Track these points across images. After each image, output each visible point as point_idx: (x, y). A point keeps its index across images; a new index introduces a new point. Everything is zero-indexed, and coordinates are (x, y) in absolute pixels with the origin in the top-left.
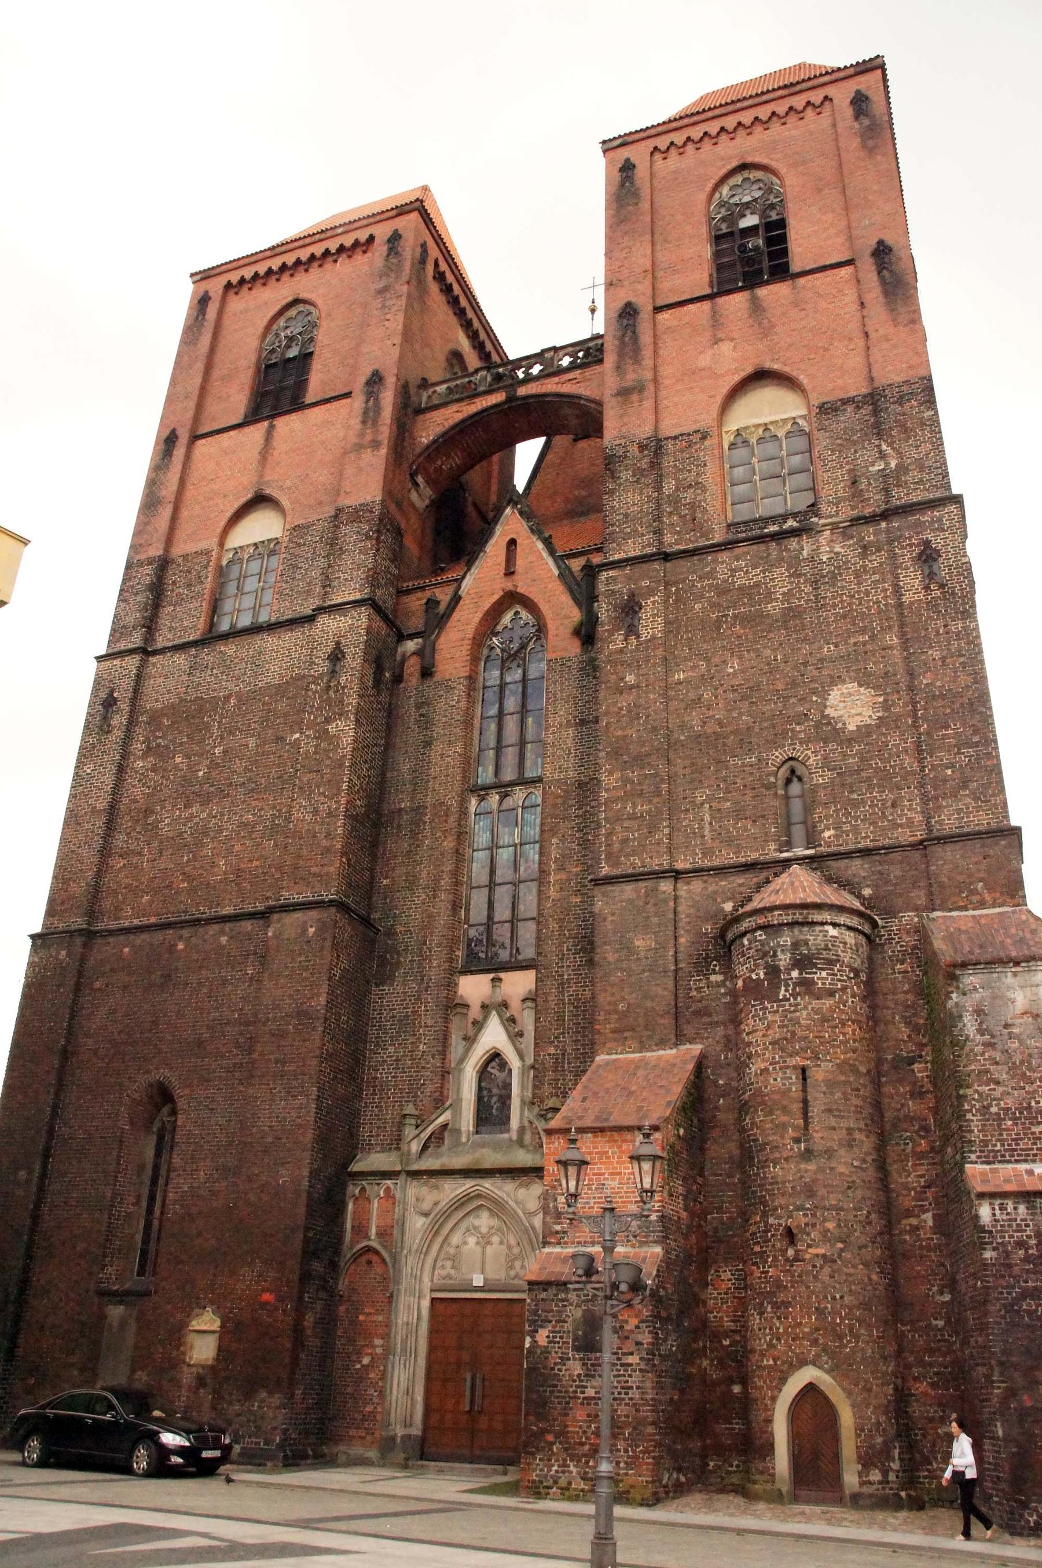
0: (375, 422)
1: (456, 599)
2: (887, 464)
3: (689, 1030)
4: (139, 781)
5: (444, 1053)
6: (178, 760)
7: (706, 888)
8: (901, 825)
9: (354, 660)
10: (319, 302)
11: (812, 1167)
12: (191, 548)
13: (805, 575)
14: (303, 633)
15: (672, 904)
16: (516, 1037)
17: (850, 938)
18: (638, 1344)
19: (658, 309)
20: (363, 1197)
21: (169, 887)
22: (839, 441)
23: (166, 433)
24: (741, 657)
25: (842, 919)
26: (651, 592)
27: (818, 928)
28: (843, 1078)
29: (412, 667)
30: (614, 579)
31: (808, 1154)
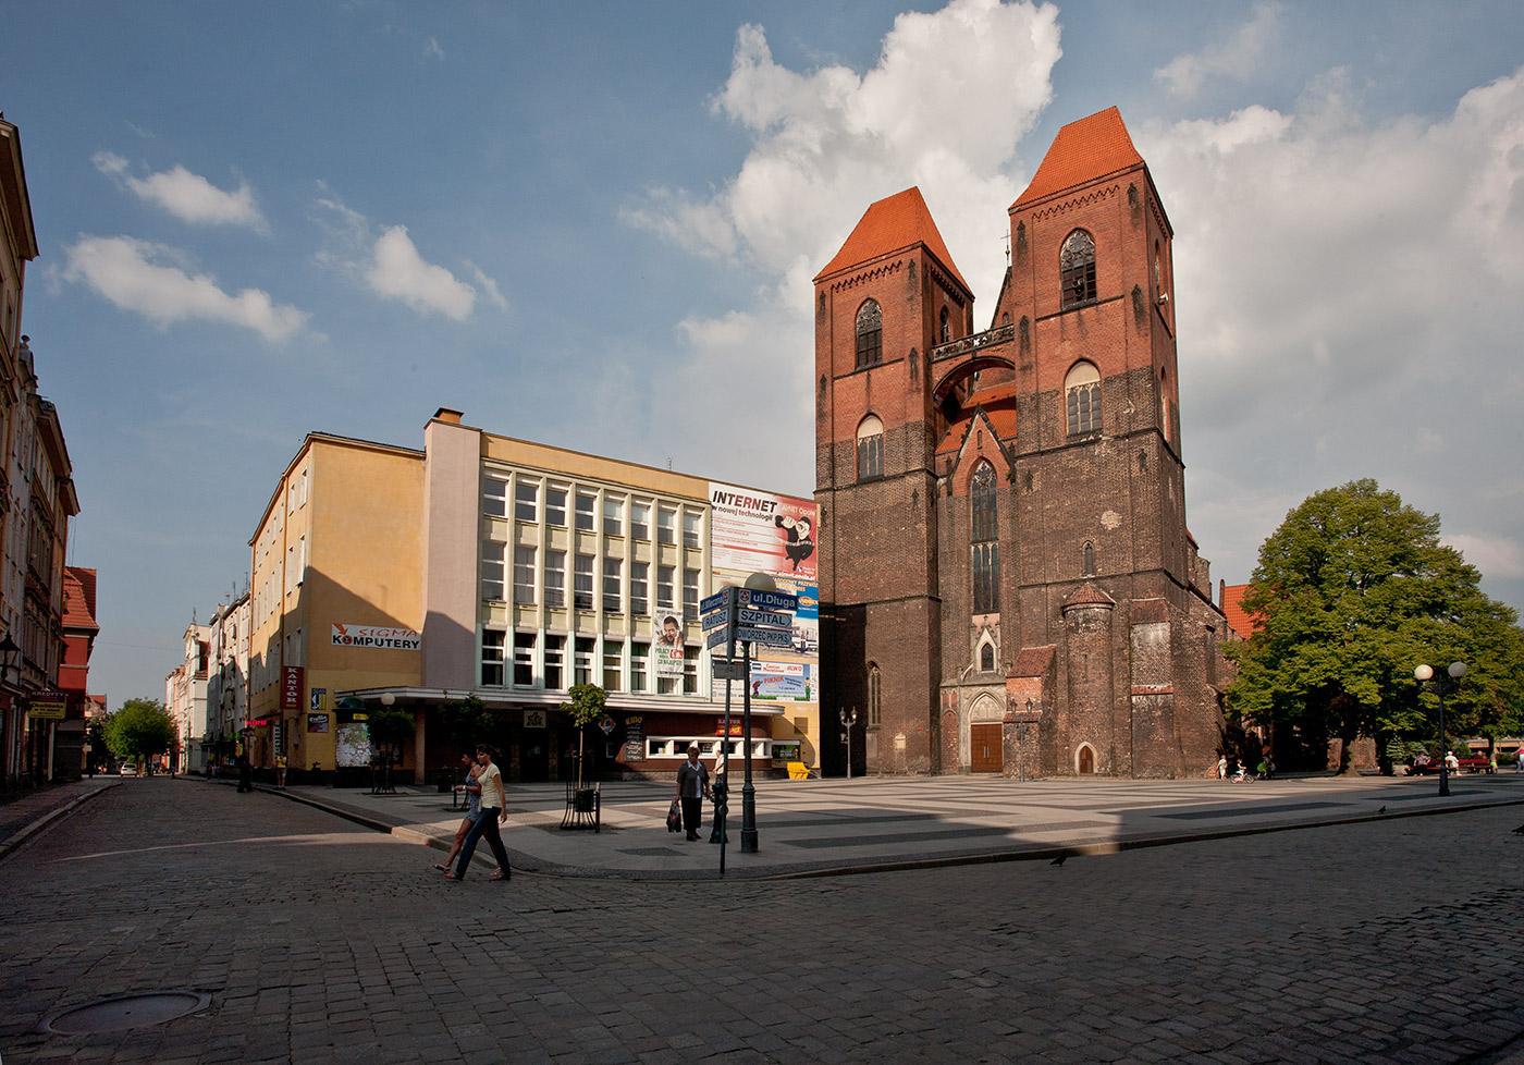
0: (917, 376)
1: (958, 459)
3: (1052, 639)
5: (969, 644)
9: (922, 497)
10: (880, 301)
16: (994, 638)
19: (1037, 320)
23: (820, 377)
25: (1100, 606)
29: (943, 490)
31: (1087, 682)
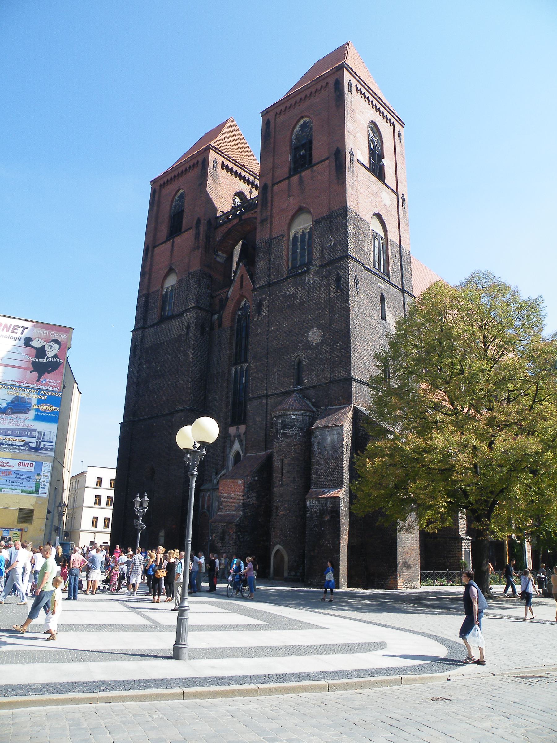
1: (227, 298)
6: (153, 364)
7: (274, 401)
8: (324, 377)
11: (282, 489)
15: (265, 406)
16: (241, 445)
17: (300, 418)
18: (233, 538)
19: (273, 185)
20: (203, 497)
22: (319, 235)
24: (287, 321)
26: (265, 299)
27: (288, 416)
28: (293, 462)
31: (282, 485)
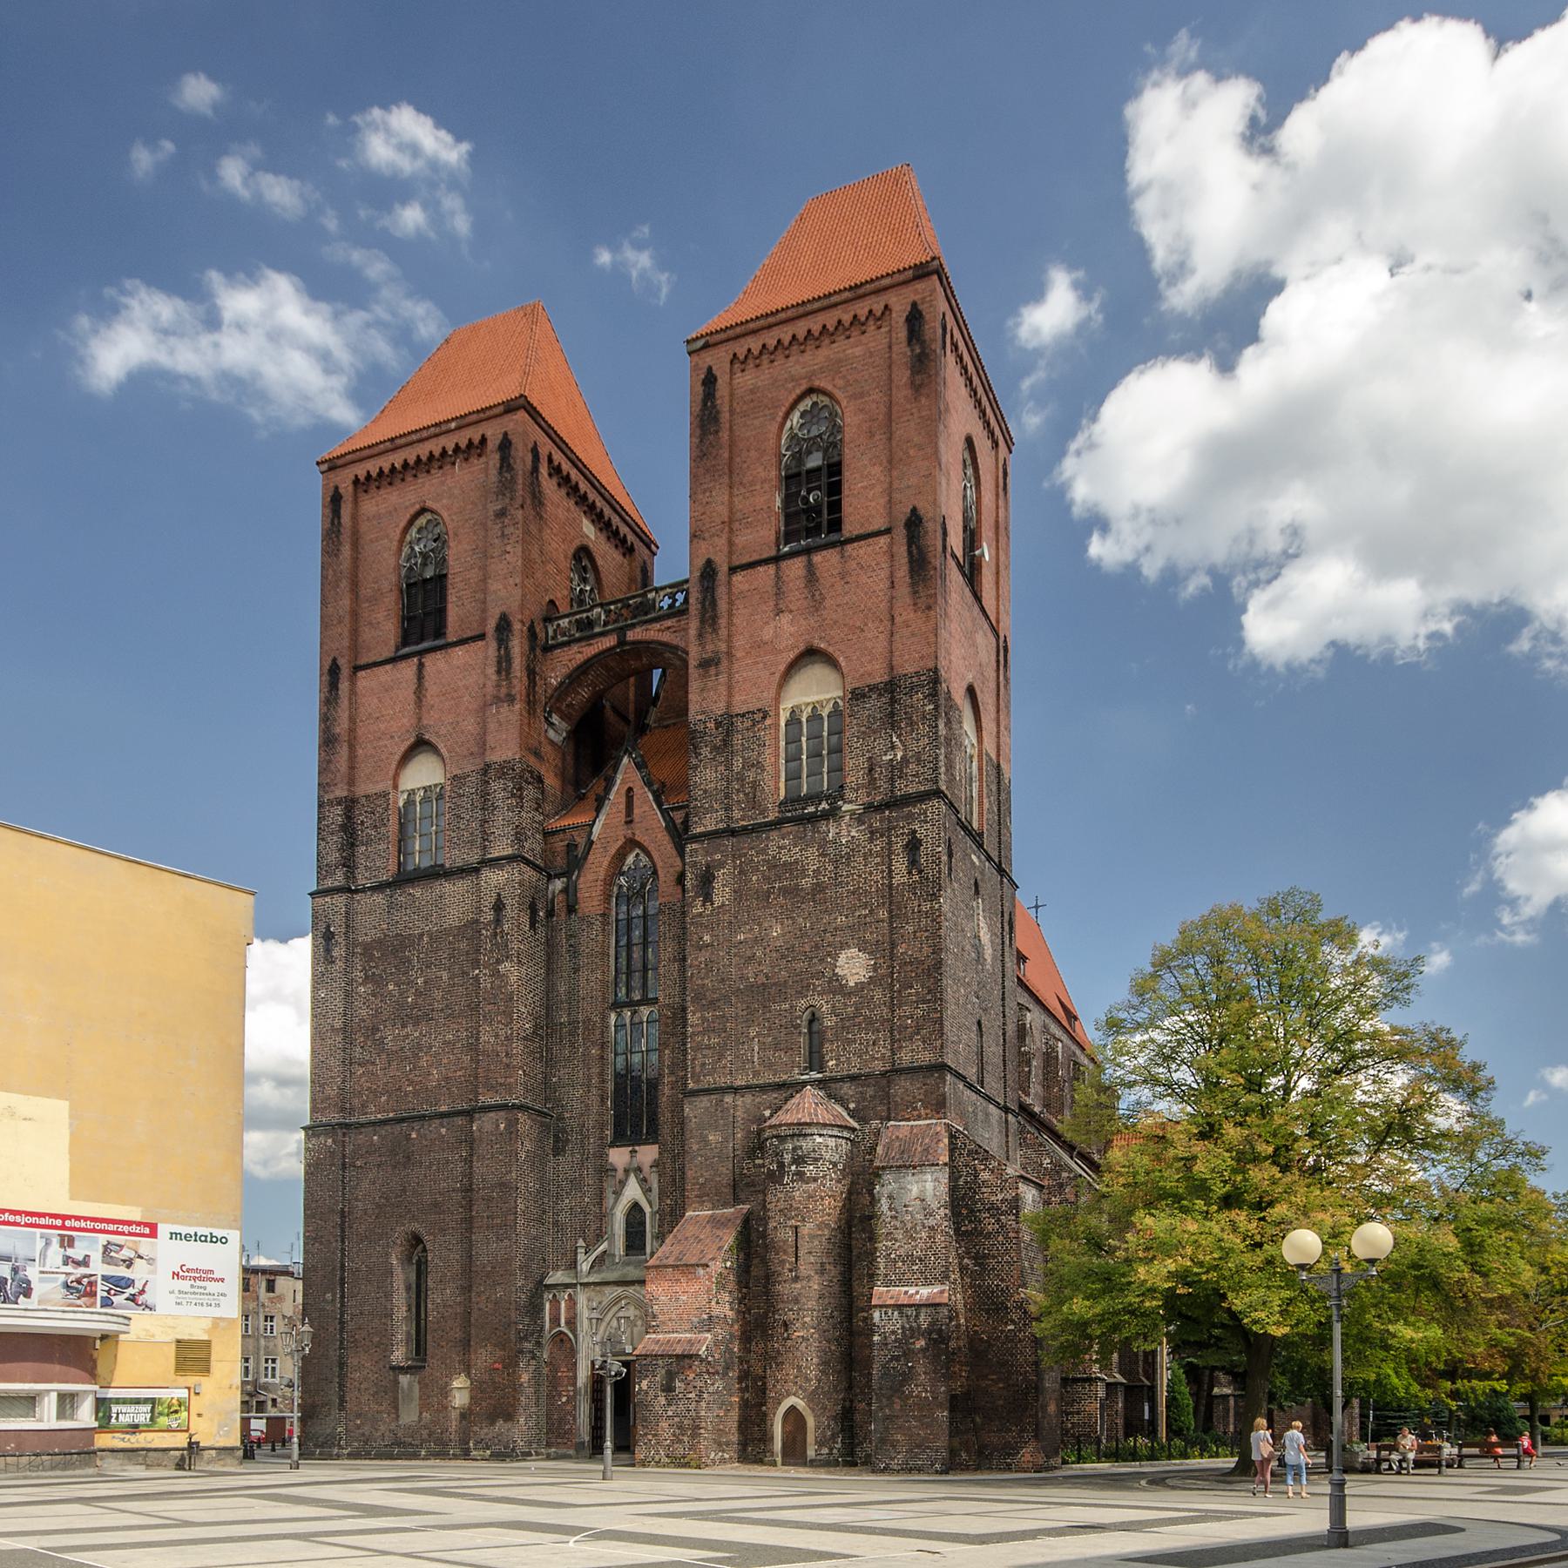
0: (508, 672)
2: (895, 755)
4: (364, 1003)
6: (391, 987)
12: (372, 789)
13: (829, 855)
14: (472, 882)
21: (399, 1089)
22: (863, 729)
26: (722, 865)
30: (696, 850)
